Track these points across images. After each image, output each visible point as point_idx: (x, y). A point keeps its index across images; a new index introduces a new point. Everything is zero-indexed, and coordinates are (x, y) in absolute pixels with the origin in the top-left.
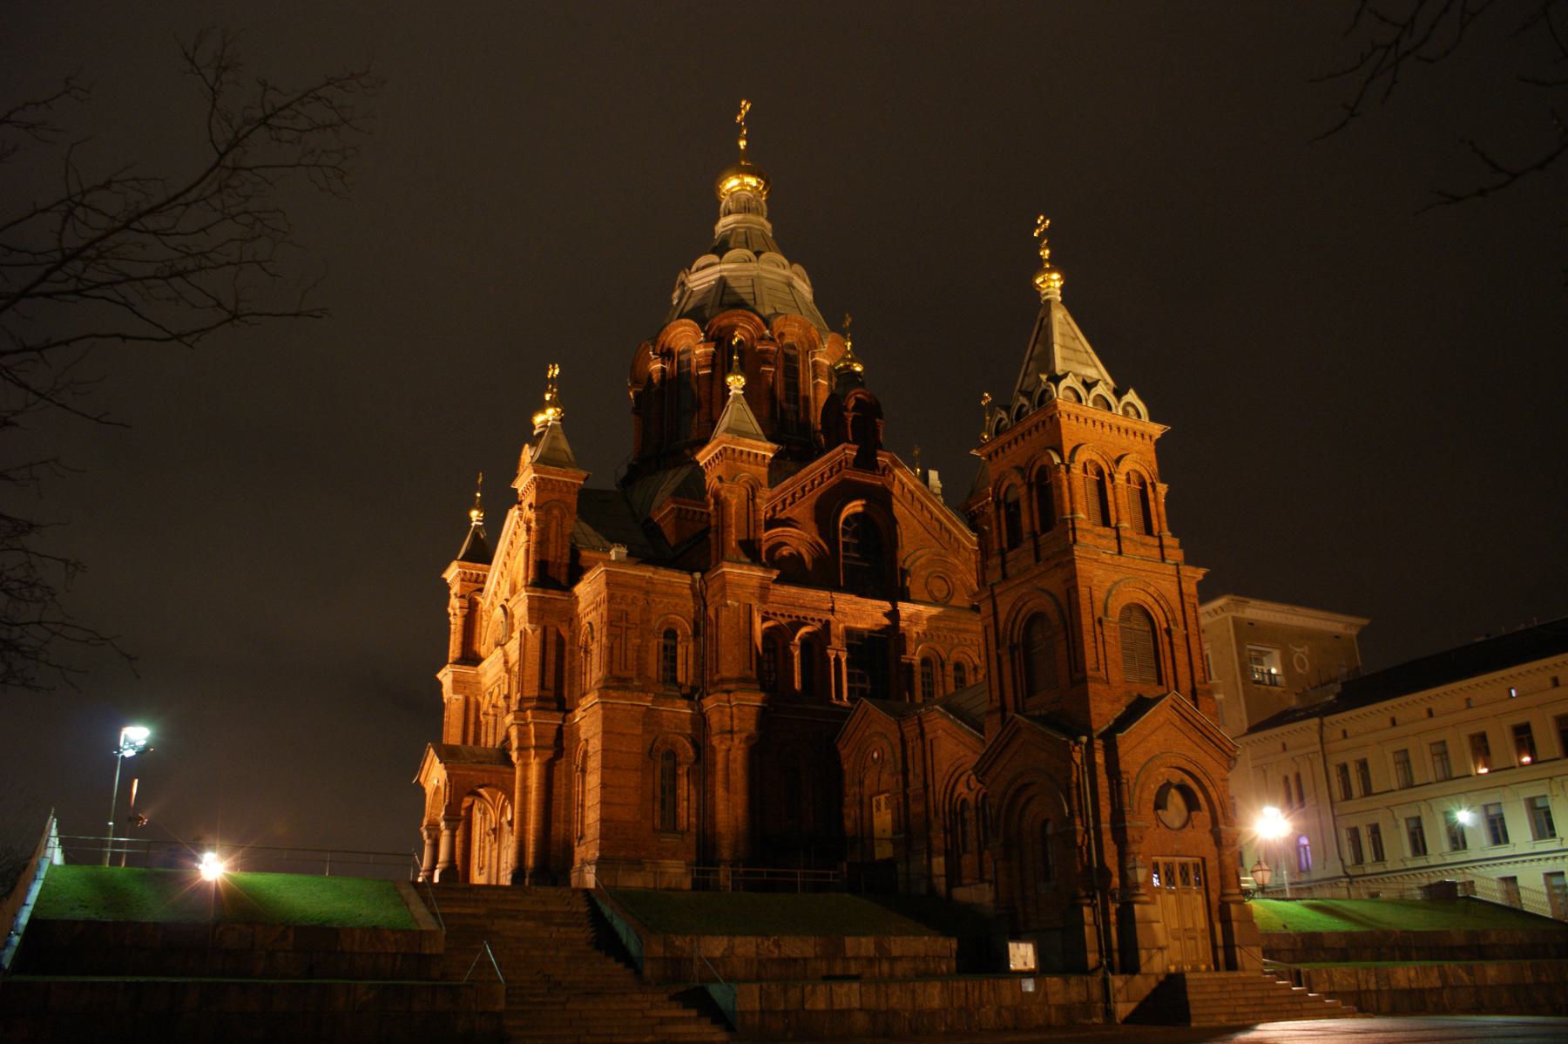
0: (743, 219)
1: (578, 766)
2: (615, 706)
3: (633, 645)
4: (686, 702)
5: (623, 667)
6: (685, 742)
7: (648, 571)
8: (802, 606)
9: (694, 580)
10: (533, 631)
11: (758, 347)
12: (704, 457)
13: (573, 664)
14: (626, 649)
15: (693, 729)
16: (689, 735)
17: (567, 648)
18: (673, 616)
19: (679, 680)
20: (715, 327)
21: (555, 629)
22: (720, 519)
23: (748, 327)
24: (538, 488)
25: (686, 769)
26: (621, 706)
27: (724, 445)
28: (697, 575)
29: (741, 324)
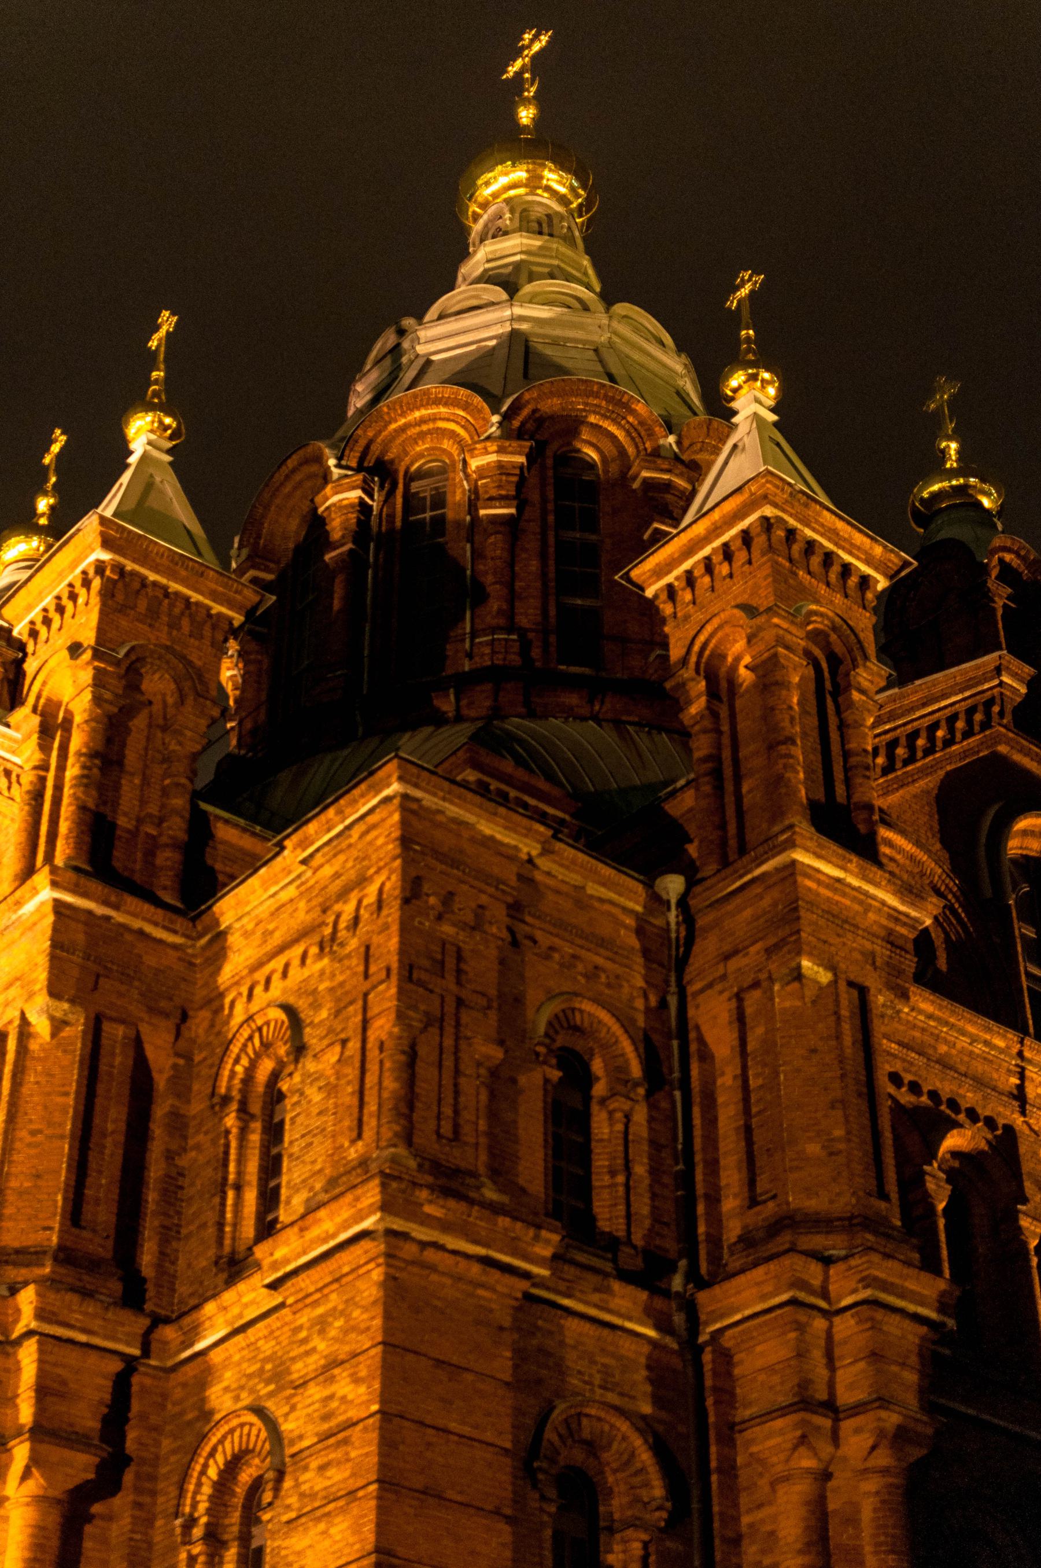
0: (540, 248)
1: (191, 1522)
2: (430, 1255)
3: (479, 1064)
4: (643, 1296)
5: (447, 1129)
6: (638, 1442)
7: (528, 833)
8: (945, 1064)
9: (657, 902)
10: (58, 1025)
11: (645, 474)
12: (660, 572)
13: (183, 1162)
14: (457, 1072)
15: (658, 1400)
16: (644, 1417)
17: (160, 1110)
18: (587, 1006)
19: (603, 1225)
20: (525, 412)
21: (132, 1034)
22: (726, 741)
23: (613, 429)
24: (107, 594)
25: (636, 1548)
26: (450, 1260)
27: (768, 511)
28: (673, 885)
29: (592, 419)
